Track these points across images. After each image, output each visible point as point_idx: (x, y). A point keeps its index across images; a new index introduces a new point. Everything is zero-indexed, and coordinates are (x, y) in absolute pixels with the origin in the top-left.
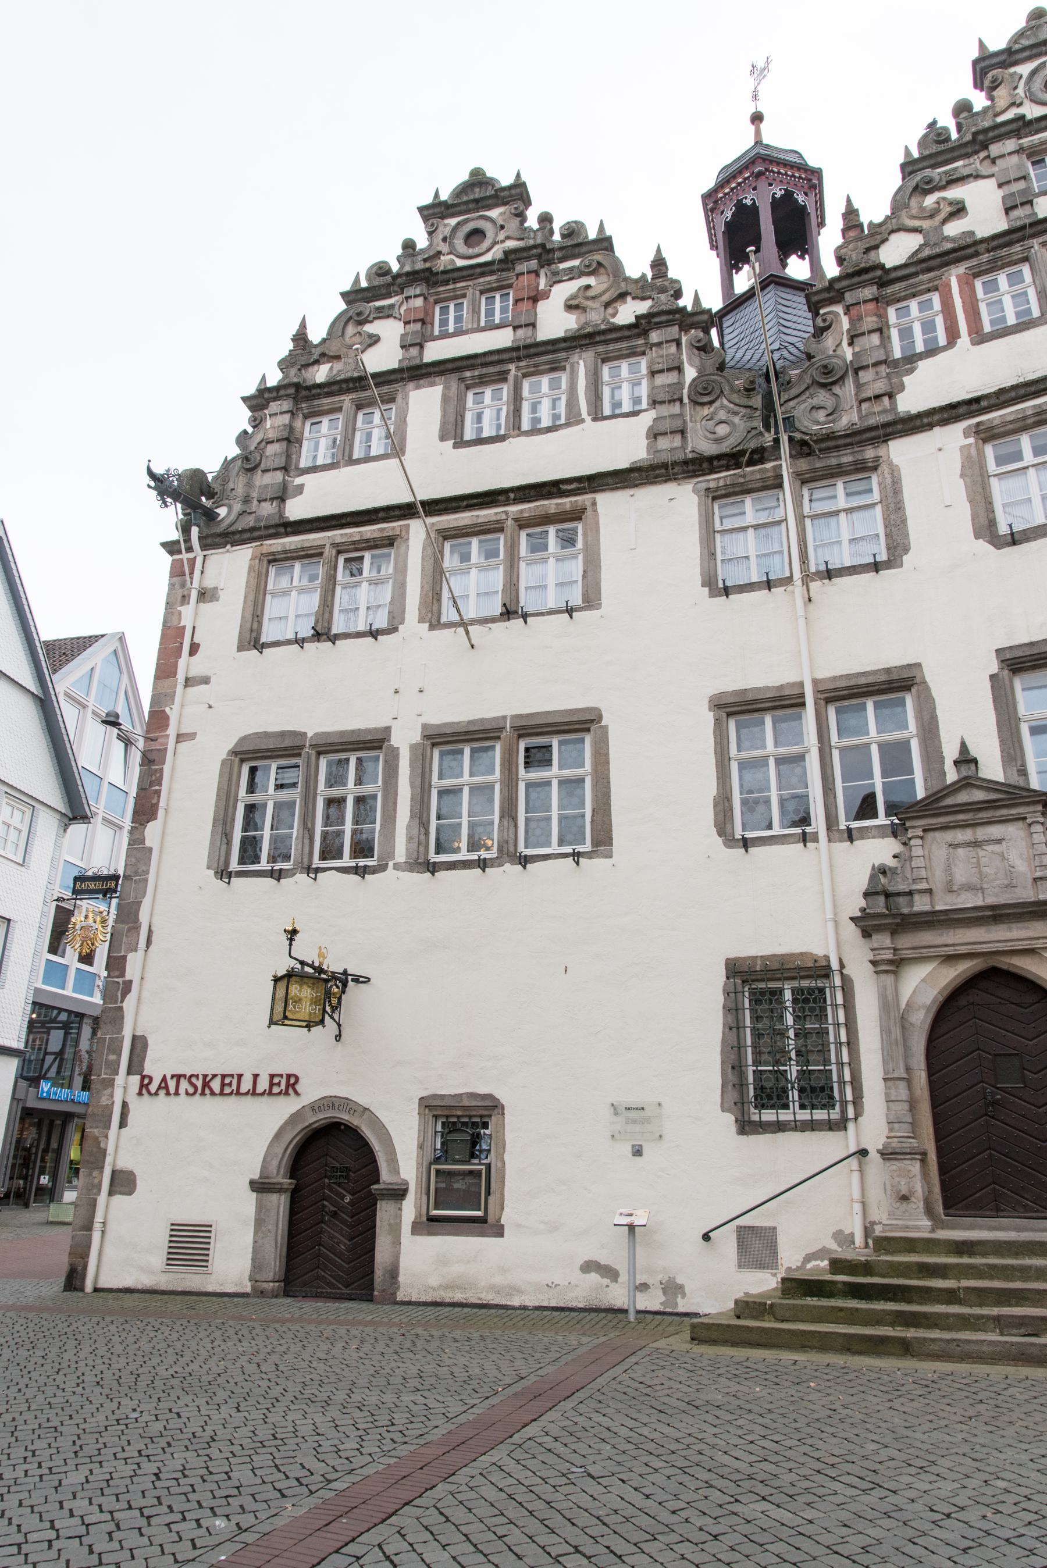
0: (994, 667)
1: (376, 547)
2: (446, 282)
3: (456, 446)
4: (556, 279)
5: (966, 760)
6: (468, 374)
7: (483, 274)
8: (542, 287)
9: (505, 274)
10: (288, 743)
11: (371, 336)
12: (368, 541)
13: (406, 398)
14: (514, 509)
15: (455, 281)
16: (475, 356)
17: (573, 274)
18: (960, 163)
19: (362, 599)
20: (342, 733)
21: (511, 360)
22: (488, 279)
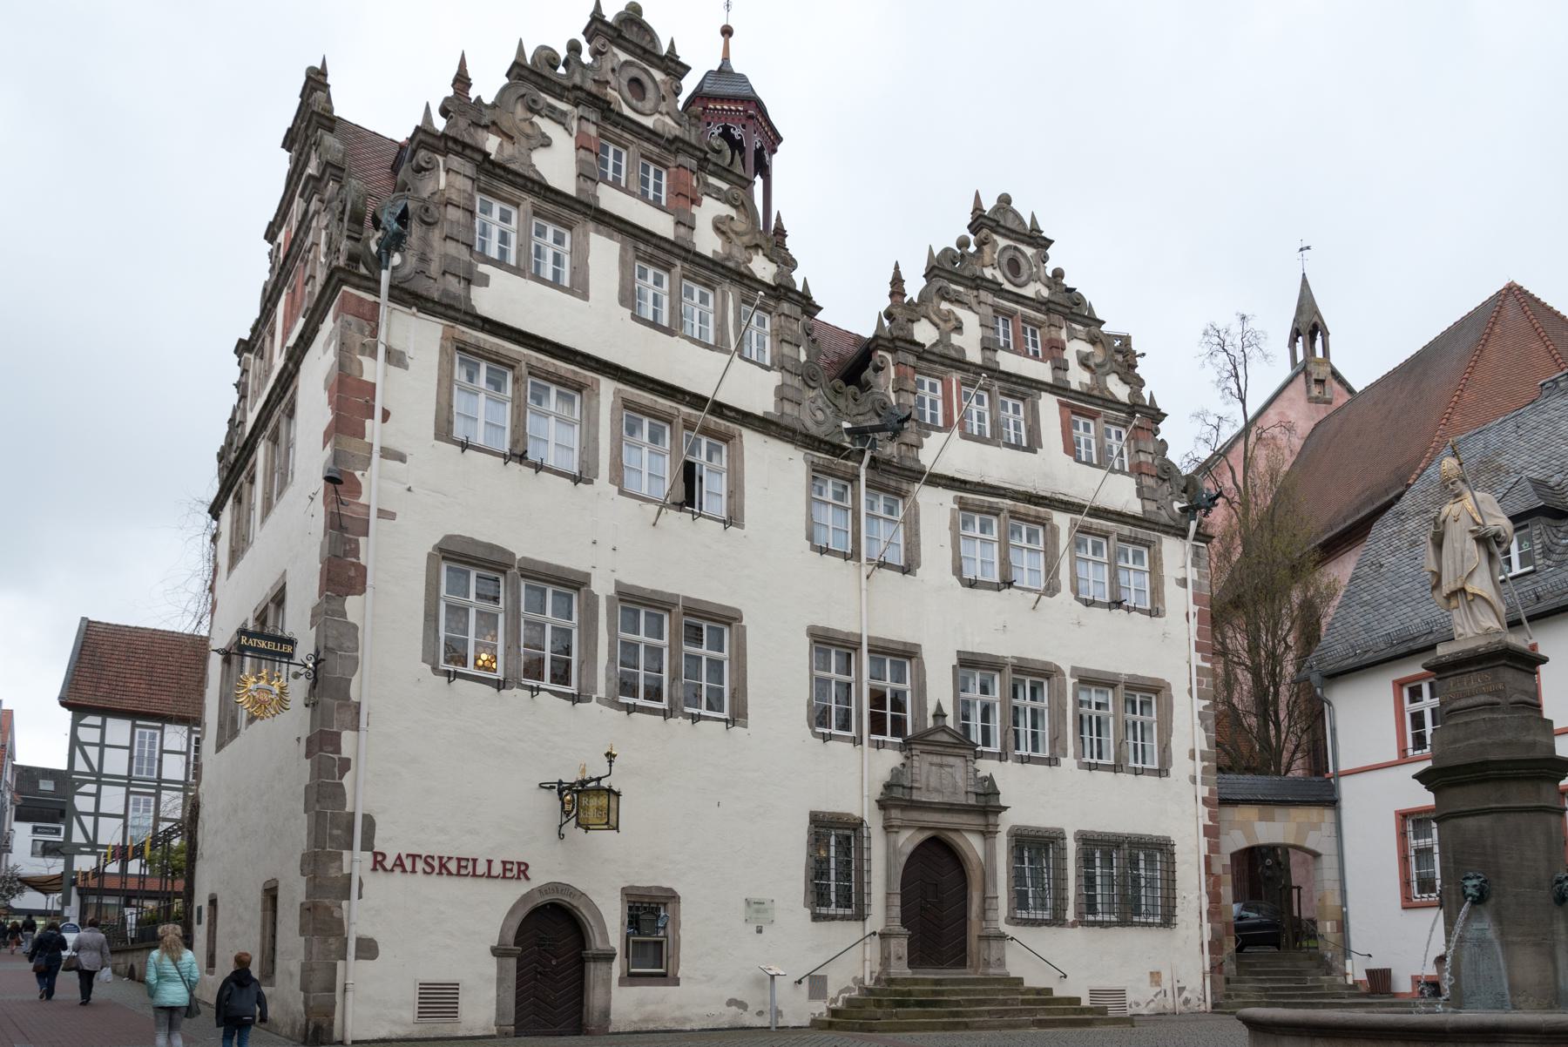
0: (955, 662)
1: (564, 385)
2: (616, 124)
6: (642, 246)
7: (648, 140)
9: (666, 154)
10: (496, 557)
12: (561, 377)
14: (685, 409)
19: (555, 434)
20: (548, 565)
21: (678, 257)
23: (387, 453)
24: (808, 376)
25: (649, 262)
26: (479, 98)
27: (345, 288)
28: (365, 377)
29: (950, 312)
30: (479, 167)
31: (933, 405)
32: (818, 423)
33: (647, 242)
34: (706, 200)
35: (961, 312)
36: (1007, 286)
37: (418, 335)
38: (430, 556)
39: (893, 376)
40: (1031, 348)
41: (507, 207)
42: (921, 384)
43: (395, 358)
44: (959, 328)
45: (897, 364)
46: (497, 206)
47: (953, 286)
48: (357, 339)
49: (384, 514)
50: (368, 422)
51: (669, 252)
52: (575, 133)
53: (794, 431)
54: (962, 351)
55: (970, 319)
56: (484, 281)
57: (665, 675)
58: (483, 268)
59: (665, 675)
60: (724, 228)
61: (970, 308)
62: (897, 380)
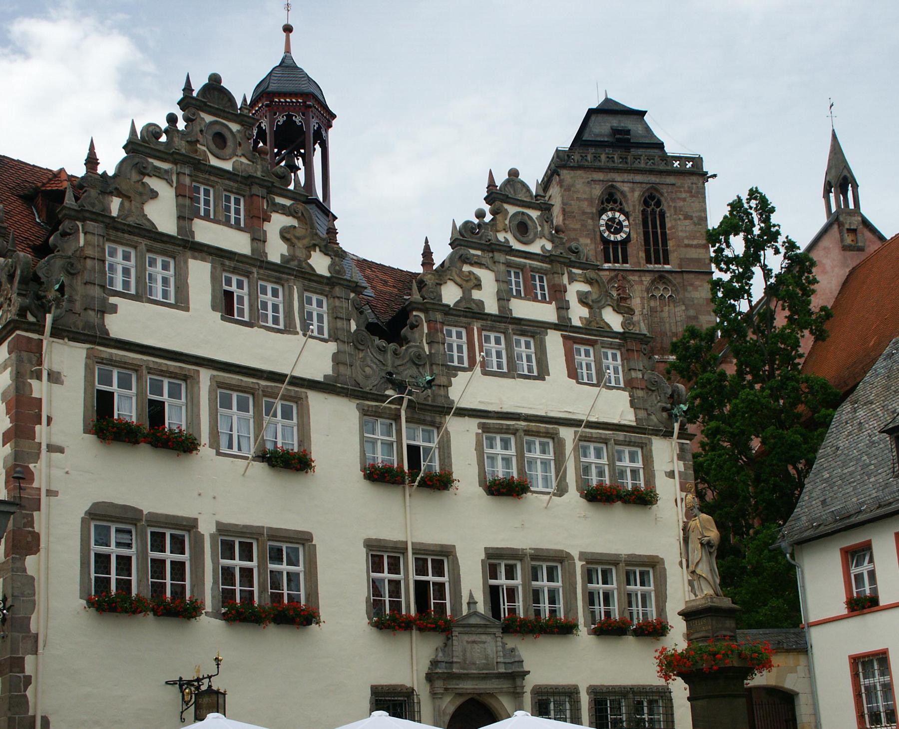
9: (243, 187)
23: (52, 448)
24: (357, 341)
25: (233, 273)
26: (105, 173)
27: (18, 332)
28: (33, 396)
29: (470, 272)
30: (107, 226)
31: (460, 348)
32: (367, 377)
33: (230, 259)
34: (275, 217)
35: (477, 271)
36: (516, 245)
37: (68, 359)
38: (83, 519)
39: (426, 331)
40: (539, 292)
41: (127, 249)
42: (450, 334)
43: (55, 378)
44: (478, 286)
45: (429, 322)
46: (120, 250)
47: (472, 252)
48: (27, 367)
49: (50, 493)
50: (37, 427)
52: (175, 185)
54: (481, 303)
55: (487, 277)
56: (114, 309)
57: (256, 589)
58: (113, 300)
59: (256, 589)
60: (288, 236)
61: (487, 268)
62: (428, 335)
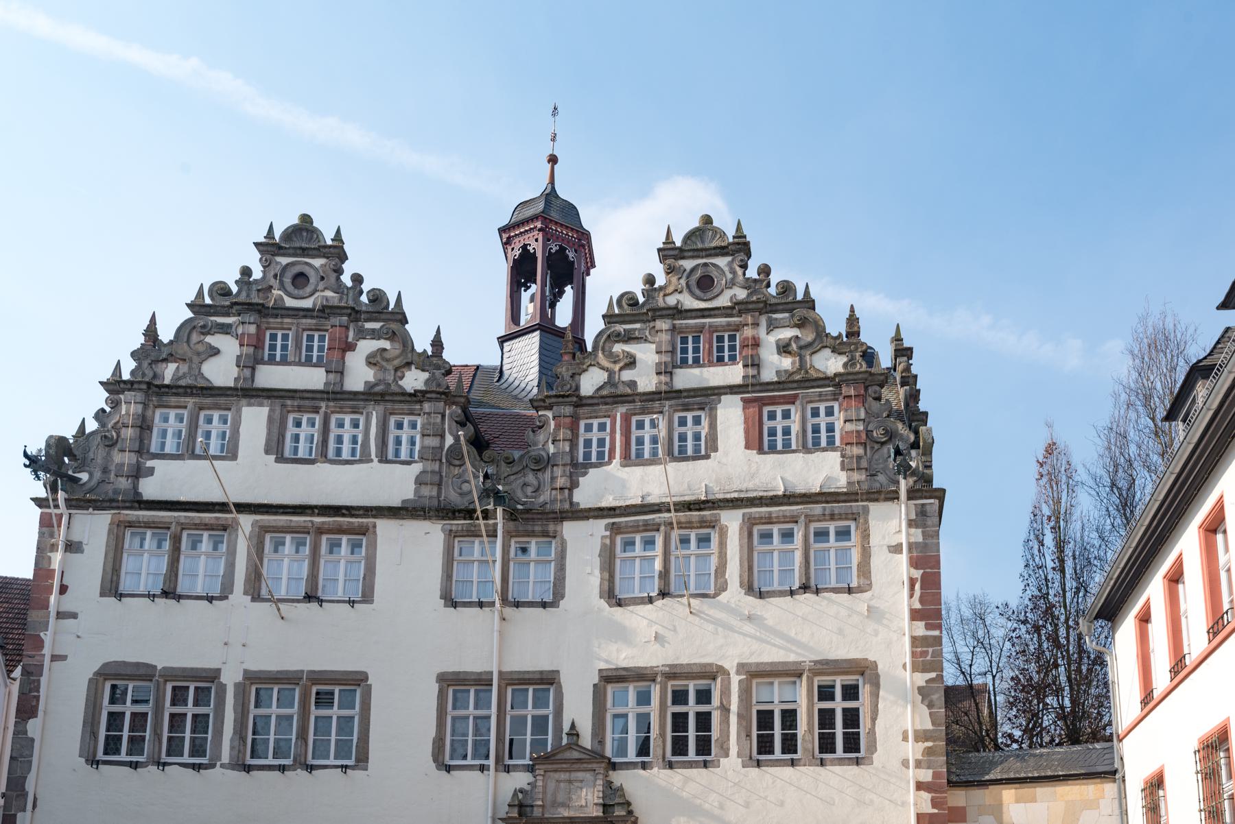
2: (276, 316)
3: (278, 460)
4: (363, 334)
5: (574, 733)
6: (289, 402)
7: (305, 317)
8: (350, 340)
11: (211, 347)
13: (239, 412)
15: (283, 316)
16: (295, 391)
17: (375, 335)
18: (638, 326)
21: (322, 399)
22: (309, 321)
51: (313, 399)
53: (423, 509)
